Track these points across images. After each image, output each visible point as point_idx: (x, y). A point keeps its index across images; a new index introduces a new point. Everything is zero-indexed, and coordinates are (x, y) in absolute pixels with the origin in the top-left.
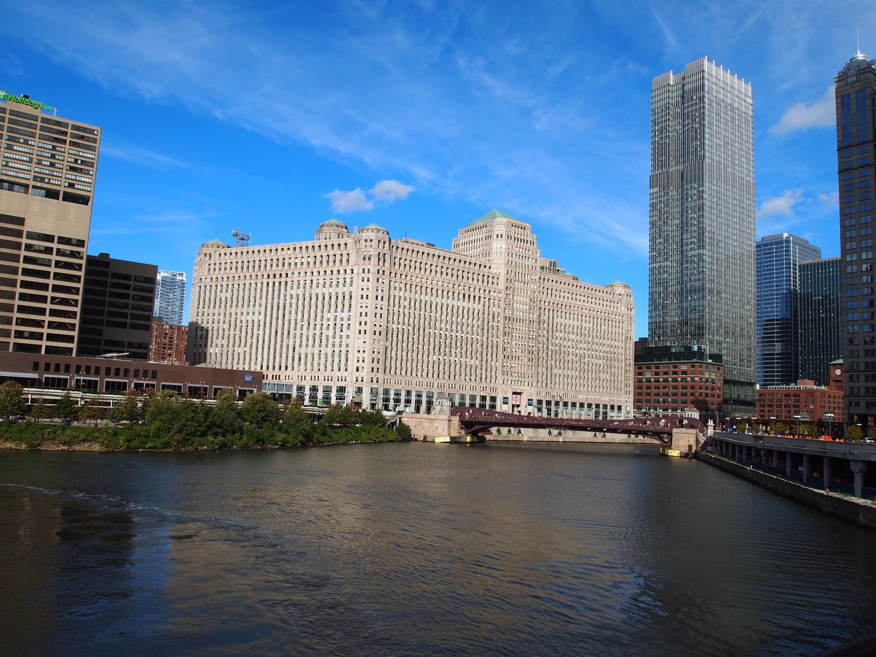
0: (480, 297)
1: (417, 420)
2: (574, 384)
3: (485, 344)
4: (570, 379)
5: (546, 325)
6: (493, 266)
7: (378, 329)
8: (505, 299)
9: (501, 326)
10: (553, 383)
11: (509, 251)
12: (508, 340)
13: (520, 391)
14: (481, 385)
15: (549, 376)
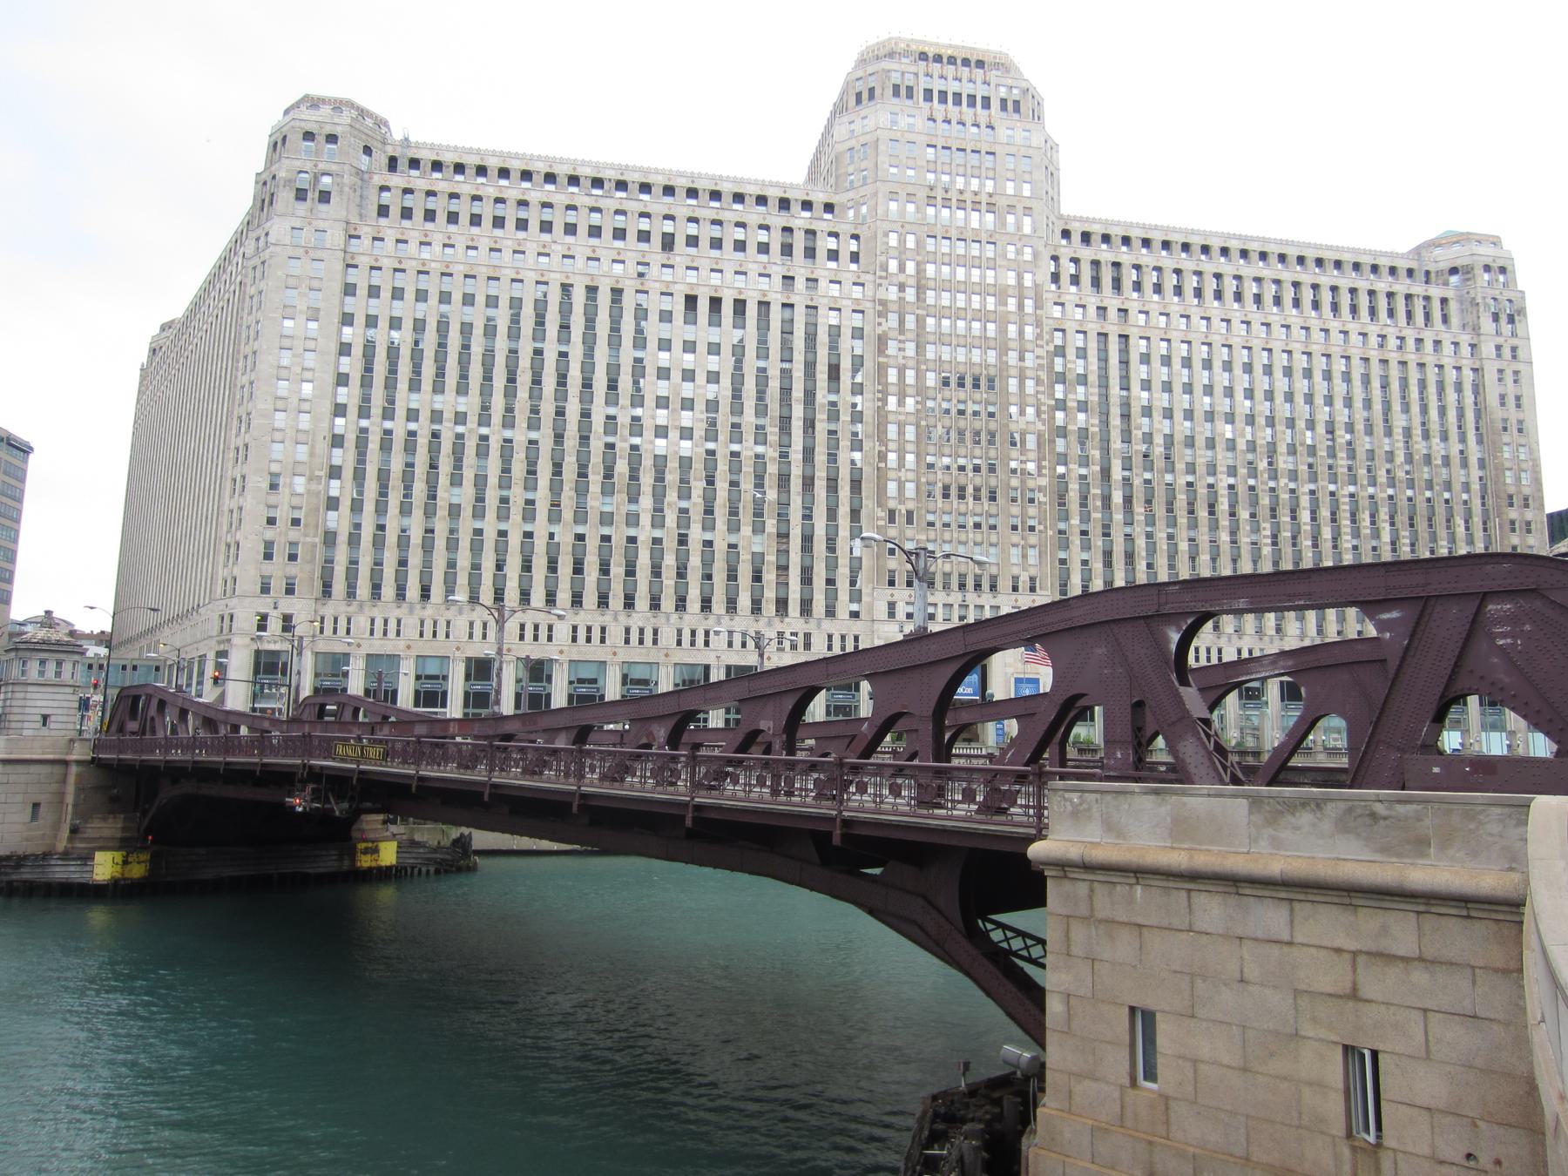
3: (796, 471)
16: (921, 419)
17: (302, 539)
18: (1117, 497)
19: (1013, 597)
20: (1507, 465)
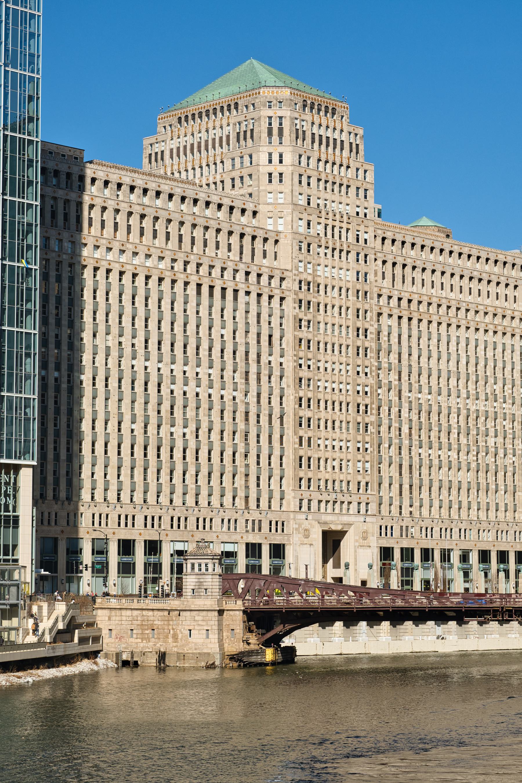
0: (236, 291)
1: (136, 613)
2: (465, 504)
4: (454, 492)
5: (394, 357)
6: (262, 209)
8: (296, 294)
9: (289, 364)
10: (417, 504)
11: (302, 171)
13: (339, 528)
14: (247, 516)
15: (406, 487)
18: (405, 429)
19: (358, 496)
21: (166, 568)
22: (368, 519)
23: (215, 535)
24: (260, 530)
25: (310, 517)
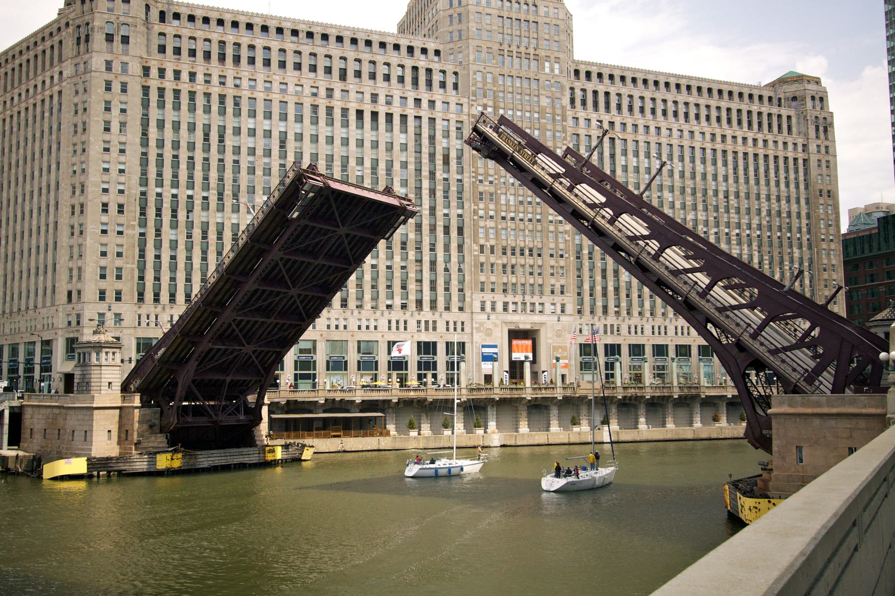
0: (404, 117)
7: (113, 200)
12: (486, 209)
13: (528, 327)
16: (498, 189)
17: (125, 265)
20: (822, 217)
21: (321, 366)
22: (562, 318)
23: (380, 335)
24: (435, 329)
25: (493, 317)
